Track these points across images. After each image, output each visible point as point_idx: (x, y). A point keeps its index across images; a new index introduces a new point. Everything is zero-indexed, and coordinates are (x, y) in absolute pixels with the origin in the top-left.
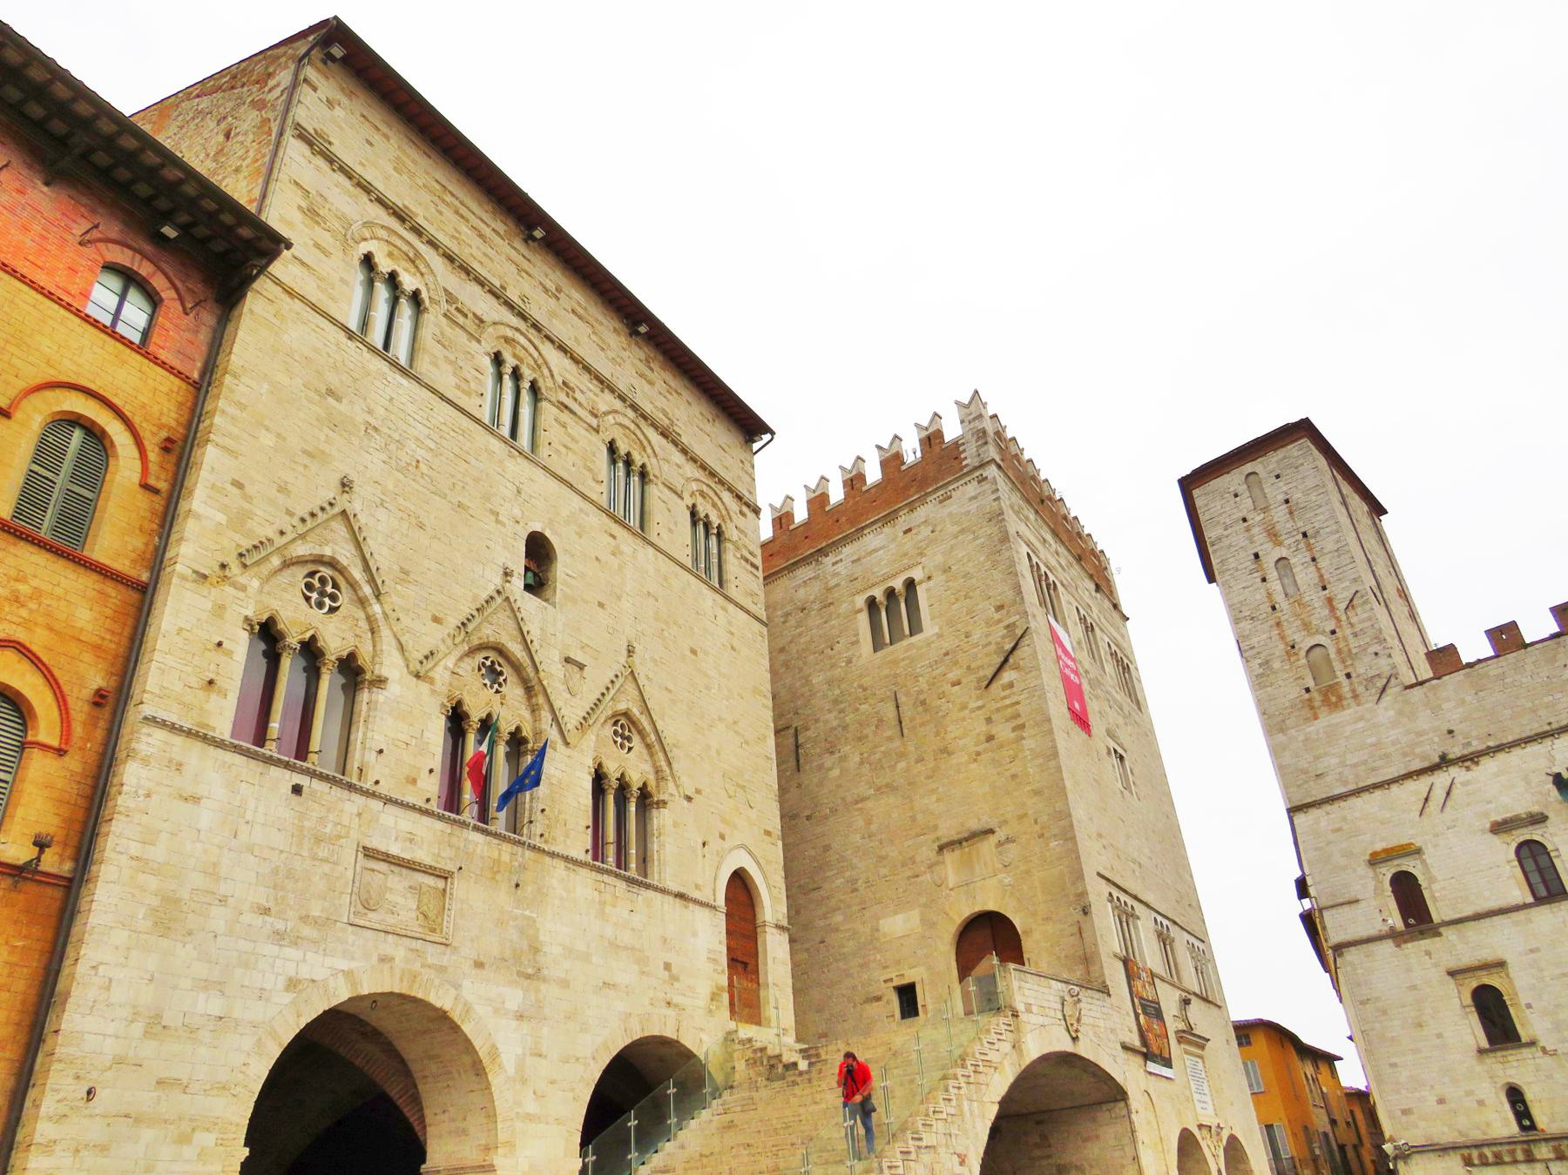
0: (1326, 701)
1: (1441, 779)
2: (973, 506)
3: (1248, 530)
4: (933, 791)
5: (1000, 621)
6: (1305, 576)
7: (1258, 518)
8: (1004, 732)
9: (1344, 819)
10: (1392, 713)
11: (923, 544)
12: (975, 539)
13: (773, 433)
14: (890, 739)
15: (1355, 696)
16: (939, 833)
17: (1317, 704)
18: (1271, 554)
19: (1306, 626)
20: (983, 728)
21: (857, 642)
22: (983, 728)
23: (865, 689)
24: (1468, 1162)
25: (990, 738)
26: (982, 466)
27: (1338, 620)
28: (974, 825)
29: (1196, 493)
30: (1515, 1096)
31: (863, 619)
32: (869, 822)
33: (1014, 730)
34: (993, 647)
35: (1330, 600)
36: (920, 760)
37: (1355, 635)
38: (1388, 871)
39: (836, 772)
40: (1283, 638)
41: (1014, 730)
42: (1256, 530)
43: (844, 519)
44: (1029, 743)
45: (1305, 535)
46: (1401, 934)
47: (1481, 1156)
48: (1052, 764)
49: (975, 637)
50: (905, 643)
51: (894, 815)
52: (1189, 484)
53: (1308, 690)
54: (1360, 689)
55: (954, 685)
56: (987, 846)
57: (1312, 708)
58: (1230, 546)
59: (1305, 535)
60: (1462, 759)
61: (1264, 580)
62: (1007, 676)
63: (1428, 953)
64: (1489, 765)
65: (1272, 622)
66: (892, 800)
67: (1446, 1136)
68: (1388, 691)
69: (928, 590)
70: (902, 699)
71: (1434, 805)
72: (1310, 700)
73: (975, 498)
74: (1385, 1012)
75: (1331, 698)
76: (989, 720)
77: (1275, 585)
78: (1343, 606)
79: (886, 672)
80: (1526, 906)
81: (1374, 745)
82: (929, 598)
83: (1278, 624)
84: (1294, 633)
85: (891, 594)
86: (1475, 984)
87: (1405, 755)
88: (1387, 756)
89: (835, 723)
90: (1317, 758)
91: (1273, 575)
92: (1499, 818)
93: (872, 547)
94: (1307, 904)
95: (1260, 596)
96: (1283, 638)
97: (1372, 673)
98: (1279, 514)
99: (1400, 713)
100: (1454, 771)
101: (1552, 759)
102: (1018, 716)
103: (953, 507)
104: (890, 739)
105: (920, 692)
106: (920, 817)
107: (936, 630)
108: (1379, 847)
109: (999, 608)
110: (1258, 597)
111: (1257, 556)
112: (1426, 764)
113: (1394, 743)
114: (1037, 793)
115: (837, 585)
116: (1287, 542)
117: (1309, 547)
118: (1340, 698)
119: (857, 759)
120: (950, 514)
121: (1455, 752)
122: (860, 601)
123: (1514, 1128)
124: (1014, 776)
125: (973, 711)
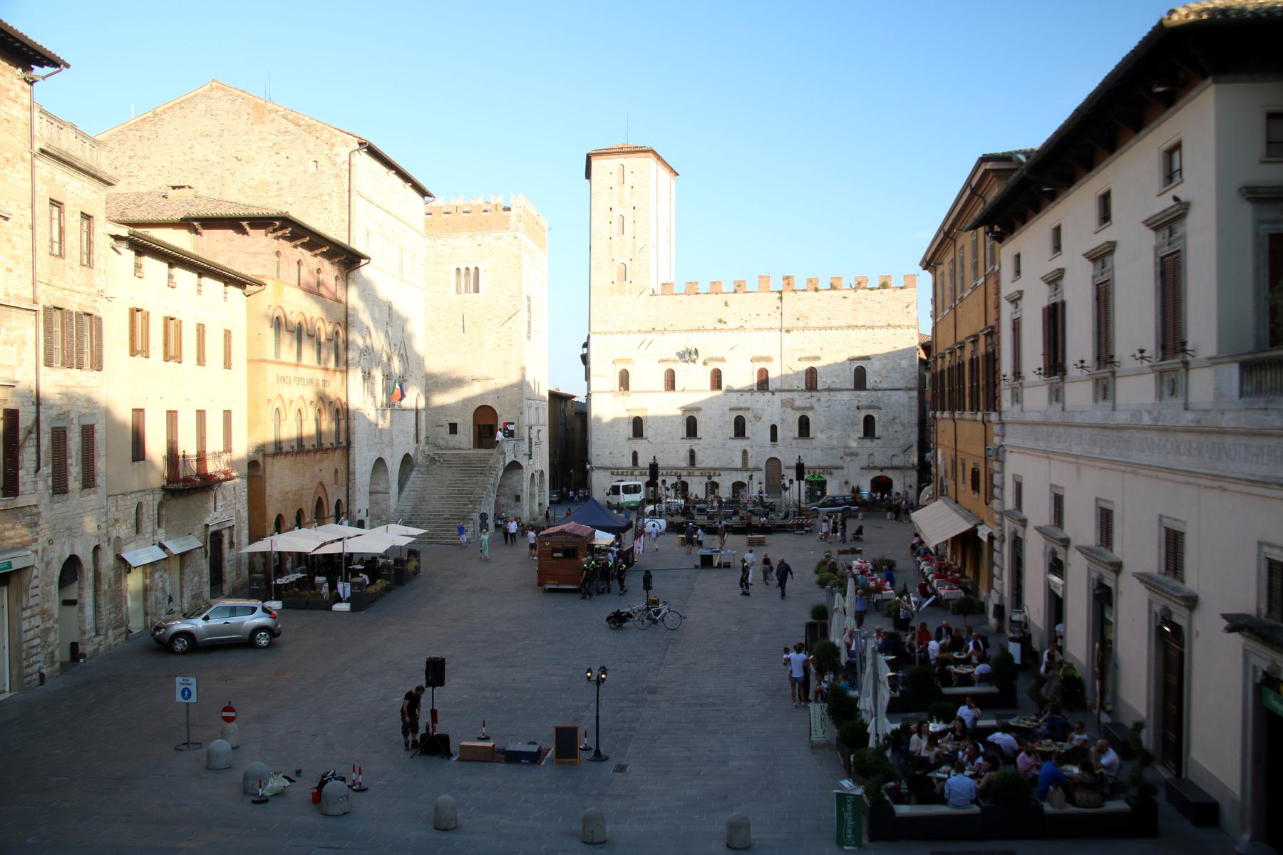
1: (649, 337)
18: (616, 213)
29: (594, 163)
30: (635, 455)
38: (620, 367)
62: (510, 324)
67: (609, 465)
85: (467, 269)
91: (616, 223)
100: (654, 335)
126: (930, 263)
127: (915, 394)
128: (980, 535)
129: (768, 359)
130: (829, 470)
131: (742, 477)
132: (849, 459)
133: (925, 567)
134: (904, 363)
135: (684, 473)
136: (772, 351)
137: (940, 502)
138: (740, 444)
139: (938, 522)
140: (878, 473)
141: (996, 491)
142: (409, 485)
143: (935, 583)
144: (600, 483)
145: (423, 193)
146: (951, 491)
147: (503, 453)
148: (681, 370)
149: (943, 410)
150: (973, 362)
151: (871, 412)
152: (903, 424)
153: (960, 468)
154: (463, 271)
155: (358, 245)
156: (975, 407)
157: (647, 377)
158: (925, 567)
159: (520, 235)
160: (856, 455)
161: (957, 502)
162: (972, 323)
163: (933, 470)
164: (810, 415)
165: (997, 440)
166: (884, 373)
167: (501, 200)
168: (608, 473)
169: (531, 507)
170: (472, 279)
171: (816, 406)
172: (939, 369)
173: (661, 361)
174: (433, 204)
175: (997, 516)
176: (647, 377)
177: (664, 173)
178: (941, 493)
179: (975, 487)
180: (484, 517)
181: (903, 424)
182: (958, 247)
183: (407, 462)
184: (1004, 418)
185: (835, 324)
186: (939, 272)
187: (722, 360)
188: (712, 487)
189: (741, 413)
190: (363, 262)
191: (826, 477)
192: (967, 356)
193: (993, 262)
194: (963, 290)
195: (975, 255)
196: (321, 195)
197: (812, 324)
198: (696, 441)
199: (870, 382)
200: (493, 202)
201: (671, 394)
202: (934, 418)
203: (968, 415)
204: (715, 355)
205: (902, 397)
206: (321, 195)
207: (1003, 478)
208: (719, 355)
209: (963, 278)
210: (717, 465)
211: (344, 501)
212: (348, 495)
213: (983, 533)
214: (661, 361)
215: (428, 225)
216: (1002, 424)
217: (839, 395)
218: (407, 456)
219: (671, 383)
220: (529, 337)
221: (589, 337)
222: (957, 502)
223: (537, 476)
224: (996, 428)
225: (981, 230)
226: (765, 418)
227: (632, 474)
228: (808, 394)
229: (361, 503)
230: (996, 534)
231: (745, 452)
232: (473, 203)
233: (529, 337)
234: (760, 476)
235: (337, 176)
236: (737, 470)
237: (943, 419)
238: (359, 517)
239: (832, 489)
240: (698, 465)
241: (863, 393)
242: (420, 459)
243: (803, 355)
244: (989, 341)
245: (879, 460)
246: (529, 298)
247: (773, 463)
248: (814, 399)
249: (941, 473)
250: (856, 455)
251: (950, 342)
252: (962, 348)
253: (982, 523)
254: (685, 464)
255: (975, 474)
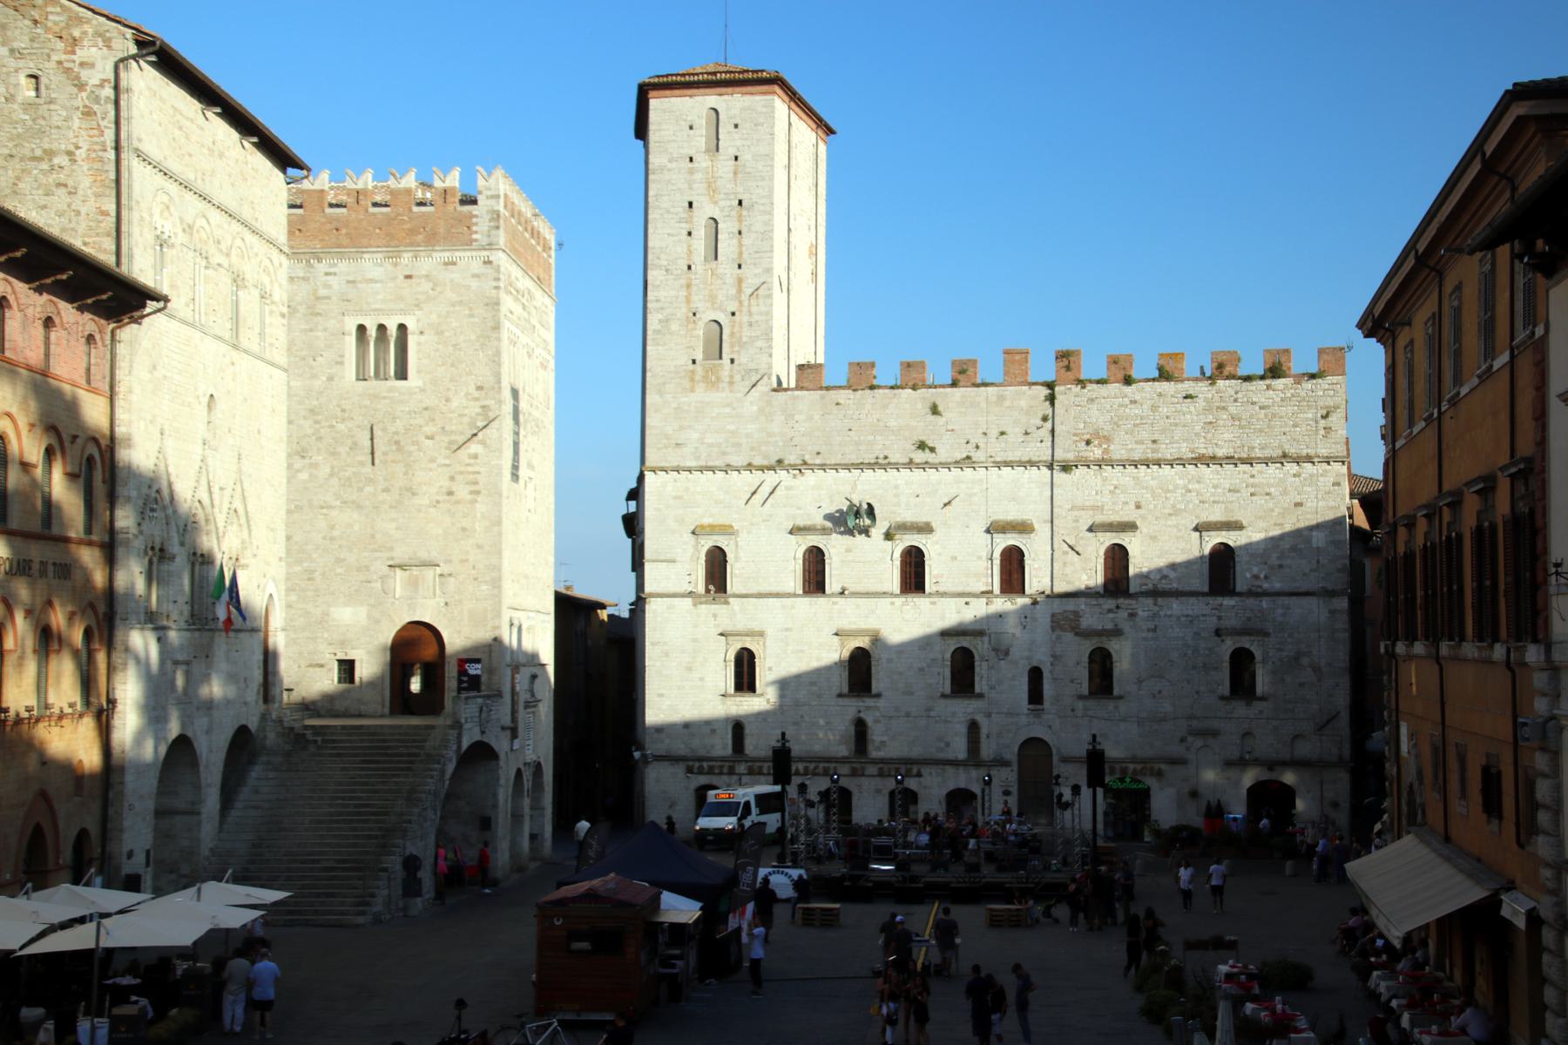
0: (705, 378)
1: (771, 478)
2: (474, 284)
3: (691, 171)
4: (393, 520)
5: (477, 399)
6: (727, 245)
7: (704, 165)
8: (462, 492)
9: (687, 490)
10: (755, 408)
11: (422, 297)
12: (472, 316)
13: (309, 170)
14: (362, 464)
15: (731, 383)
16: (394, 554)
17: (697, 378)
19: (712, 298)
20: (447, 484)
21: (342, 363)
22: (447, 484)
23: (343, 411)
24: (690, 770)
25: (450, 493)
26: (490, 246)
27: (741, 302)
28: (423, 555)
29: (654, 104)
31: (352, 340)
32: (332, 527)
33: (471, 493)
34: (466, 420)
35: (740, 281)
36: (386, 490)
37: (750, 325)
38: (707, 543)
39: (304, 476)
40: (688, 301)
41: (471, 493)
42: (698, 176)
43: (344, 231)
44: (481, 507)
45: (740, 203)
46: (700, 596)
47: (701, 767)
48: (496, 529)
49: (455, 404)
50: (389, 383)
51: (356, 527)
52: (643, 93)
53: (694, 362)
54: (737, 378)
55: (427, 438)
56: (429, 573)
57: (692, 380)
58: (669, 181)
59: (740, 203)
60: (794, 466)
61: (690, 234)
62: (474, 448)
63: (715, 616)
64: (811, 478)
65: (683, 282)
66: (356, 516)
68: (759, 387)
69: (419, 344)
70: (377, 433)
71: (759, 498)
72: (693, 372)
73: (475, 276)
74: (667, 655)
75: (712, 382)
76: (452, 479)
77: (700, 244)
78: (750, 291)
79: (367, 402)
80: (795, 595)
81: (732, 432)
82: (419, 351)
83: (689, 286)
84: (699, 303)
85: (382, 328)
86: (739, 646)
87: (752, 449)
88: (739, 445)
89: (309, 431)
90: (682, 428)
91: (701, 233)
92: (801, 523)
93: (370, 276)
94: (633, 504)
95: (681, 250)
96: (688, 301)
97: (752, 366)
98: (724, 166)
99: (761, 410)
101: (854, 486)
102: (476, 483)
103: (454, 274)
104: (362, 464)
105: (397, 433)
106: (378, 536)
107: (420, 383)
108: (707, 521)
109: (480, 388)
110: (679, 249)
111: (691, 204)
112: (766, 463)
113: (747, 436)
114: (479, 547)
115: (328, 298)
116: (722, 203)
117: (740, 219)
118: (719, 379)
119: (328, 470)
120: (452, 281)
121: (792, 459)
122: (351, 325)
123: (729, 751)
124: (464, 529)
125: (440, 466)
126: (1380, 322)
127: (1342, 603)
128: (1505, 912)
129: (1024, 528)
130: (1153, 766)
131: (967, 779)
132: (1199, 743)
133: (1380, 982)
134: (1319, 539)
135: (845, 769)
136: (1034, 511)
137: (1408, 840)
138: (963, 708)
139: (1407, 885)
140: (1265, 775)
141: (1543, 818)
142: (244, 794)
143: (1405, 1021)
144: (664, 791)
145: (282, 158)
146: (1435, 816)
147: (457, 726)
148: (836, 548)
149: (1411, 638)
150: (1483, 536)
151: (1245, 642)
152: (1316, 669)
153: (1453, 764)
154: (372, 332)
155: (141, 269)
156: (1487, 633)
157: (766, 560)
158: (1380, 982)
159: (500, 258)
160: (1214, 733)
161: (1447, 839)
162: (1479, 448)
163: (1390, 768)
164: (1114, 646)
165: (1541, 706)
166: (1274, 560)
167: (453, 180)
168: (680, 769)
169: (514, 844)
170: (389, 350)
171: (1126, 626)
172: (1401, 549)
173: (795, 530)
174: (306, 185)
175: (1547, 873)
176: (766, 560)
177: (805, 133)
178: (1412, 819)
179: (1492, 805)
180: (411, 864)
181: (1316, 669)
182: (1448, 287)
183: (242, 741)
184: (1557, 656)
185: (1167, 452)
186: (1402, 342)
187: (926, 529)
188: (904, 800)
189: (965, 642)
190: (151, 306)
191: (1150, 781)
192: (1469, 520)
193: (1531, 318)
194: (1458, 380)
195: (1489, 304)
196: (50, 154)
197: (1118, 452)
198: (870, 702)
199: (1244, 576)
200: (438, 184)
201: (819, 601)
202: (1392, 655)
203: (1470, 649)
204: (908, 516)
205: (1314, 611)
206: (50, 154)
207: (1558, 788)
208: (922, 519)
209: (1458, 354)
210: (916, 752)
211: (94, 831)
212: (105, 819)
213: (1514, 909)
214: (795, 530)
215: (295, 229)
216: (1553, 669)
217: (1176, 606)
218: (242, 731)
219: (815, 576)
220: (515, 477)
221: (641, 478)
222: (1447, 839)
223: (527, 776)
224: (1540, 680)
225: (1504, 251)
226: (1015, 653)
227: (731, 772)
228: (1110, 603)
229: (136, 836)
230: (1546, 912)
231: (973, 727)
232: (392, 183)
233: (515, 477)
234: (1007, 777)
235: (88, 113)
236: (955, 763)
237: (1410, 657)
238: (128, 868)
239: (1165, 808)
240: (874, 754)
241: (1228, 602)
242: (271, 737)
243: (1100, 518)
244: (1521, 489)
245: (1265, 745)
246: (515, 393)
247: (1034, 752)
248: (1124, 614)
249: (1409, 775)
250: (1214, 733)
251: (1427, 492)
252: (1456, 505)
253: (1510, 887)
254: (843, 751)
255: (1491, 779)
